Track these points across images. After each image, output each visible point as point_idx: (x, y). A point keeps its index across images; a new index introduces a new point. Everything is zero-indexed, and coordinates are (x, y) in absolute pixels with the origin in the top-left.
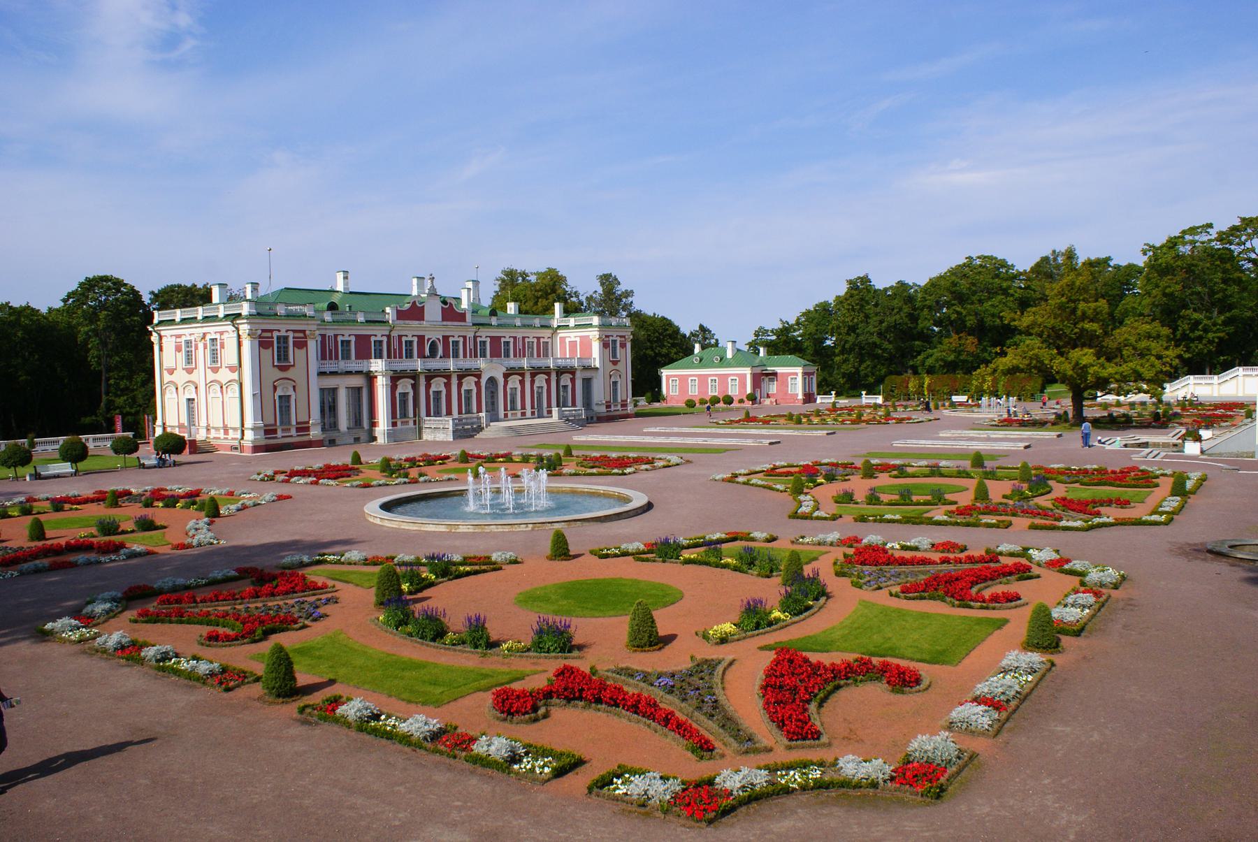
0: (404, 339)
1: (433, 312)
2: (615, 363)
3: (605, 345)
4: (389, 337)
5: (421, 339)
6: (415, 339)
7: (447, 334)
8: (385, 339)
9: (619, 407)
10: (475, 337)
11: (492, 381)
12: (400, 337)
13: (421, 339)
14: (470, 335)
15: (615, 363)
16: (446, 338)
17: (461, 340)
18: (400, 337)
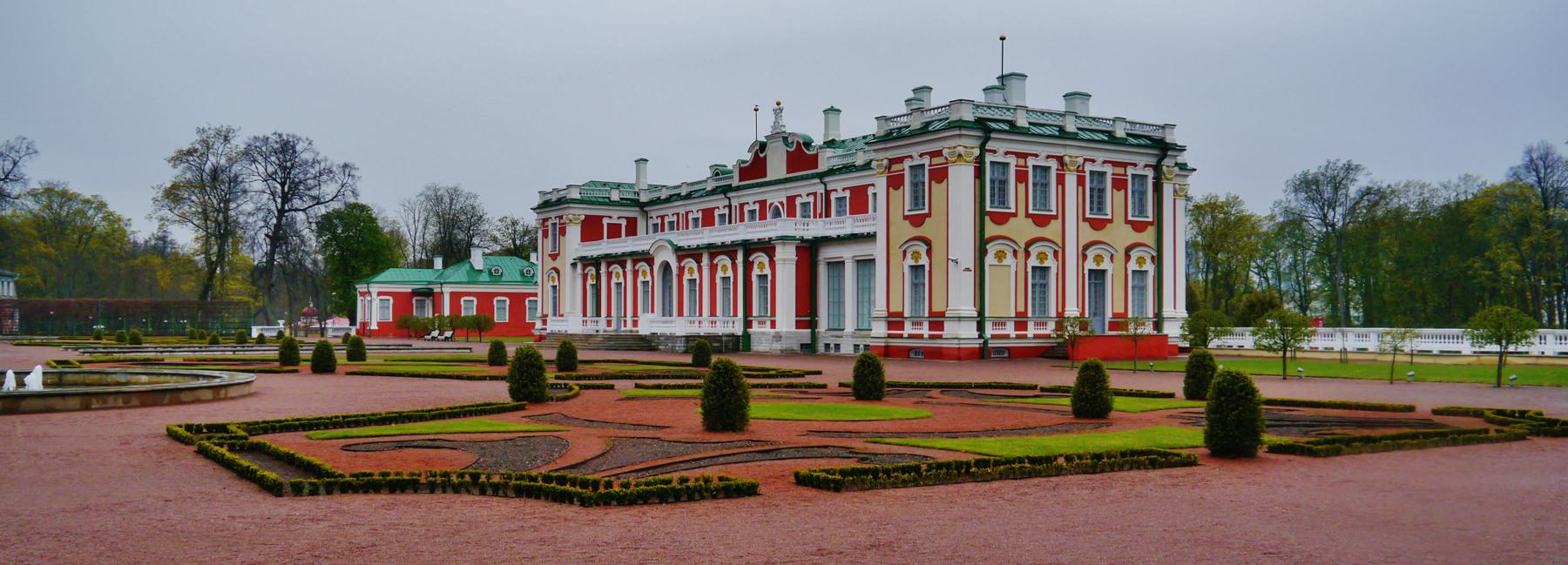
0: (746, 208)
1: (777, 167)
2: (917, 221)
3: (895, 182)
4: (730, 206)
5: (763, 203)
6: (757, 207)
7: (792, 193)
8: (726, 211)
9: (925, 331)
10: (828, 193)
11: (666, 267)
12: (742, 205)
13: (763, 203)
14: (820, 189)
15: (917, 221)
16: (791, 200)
17: (811, 199)
18: (742, 205)
